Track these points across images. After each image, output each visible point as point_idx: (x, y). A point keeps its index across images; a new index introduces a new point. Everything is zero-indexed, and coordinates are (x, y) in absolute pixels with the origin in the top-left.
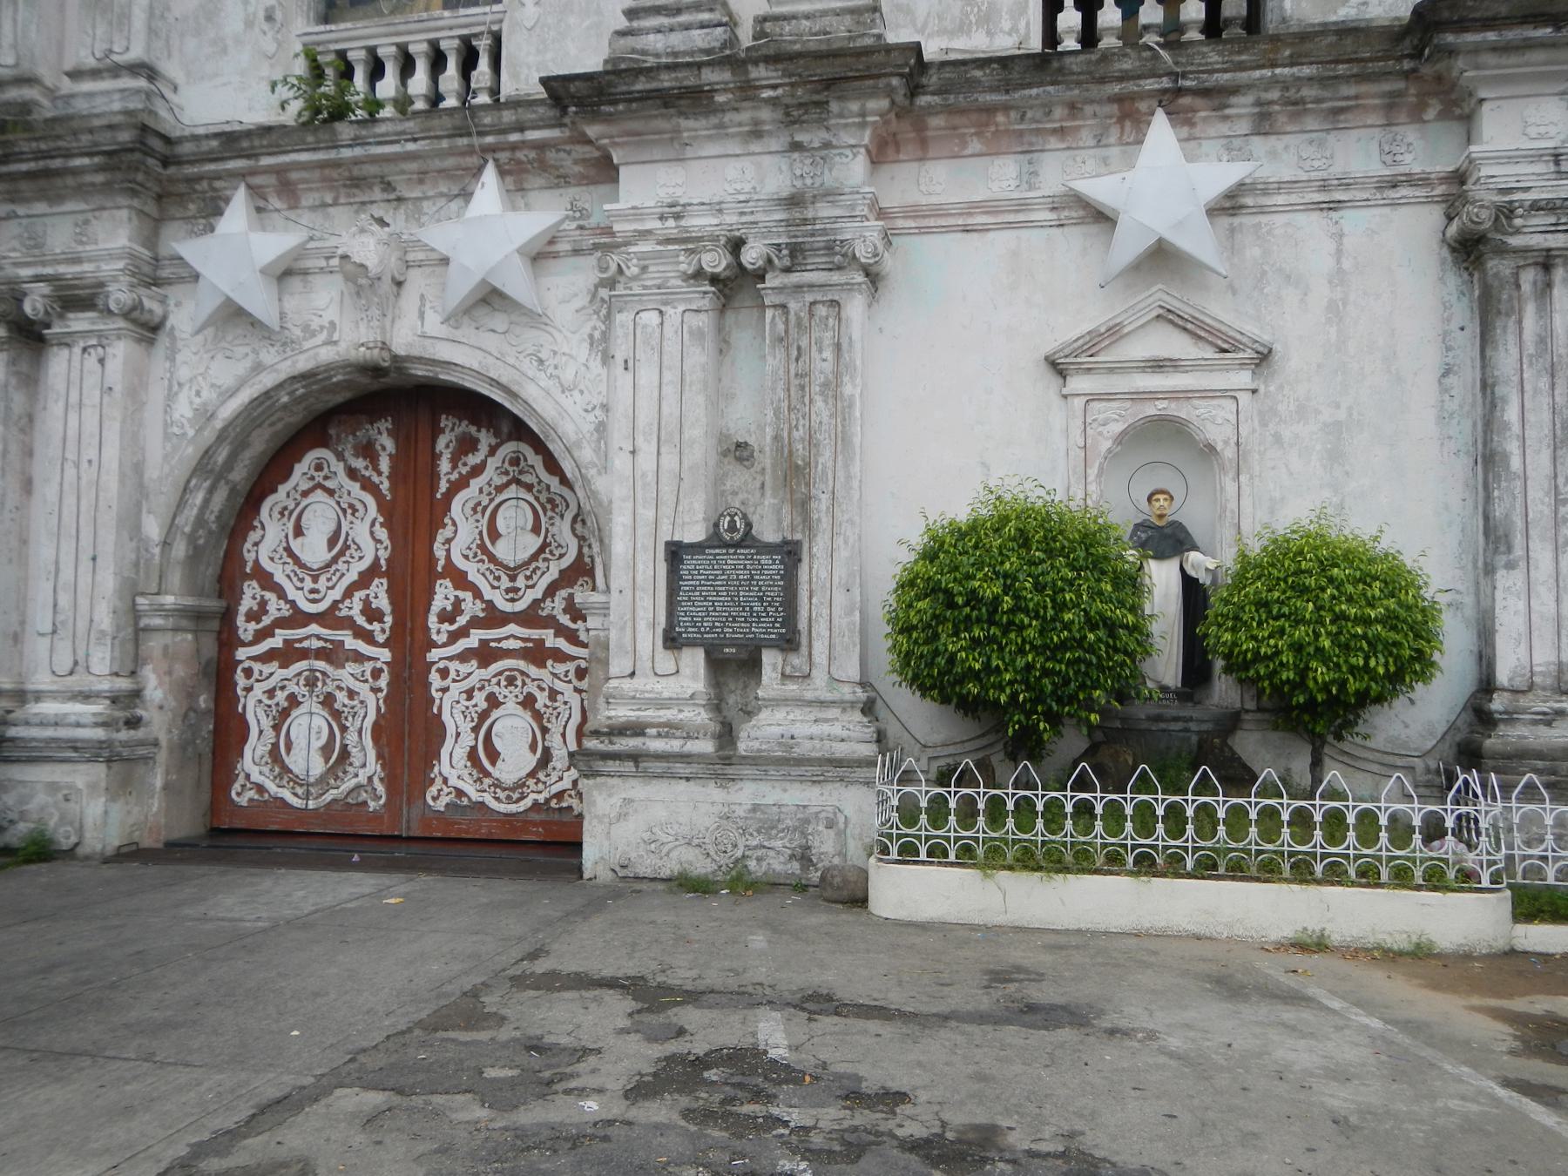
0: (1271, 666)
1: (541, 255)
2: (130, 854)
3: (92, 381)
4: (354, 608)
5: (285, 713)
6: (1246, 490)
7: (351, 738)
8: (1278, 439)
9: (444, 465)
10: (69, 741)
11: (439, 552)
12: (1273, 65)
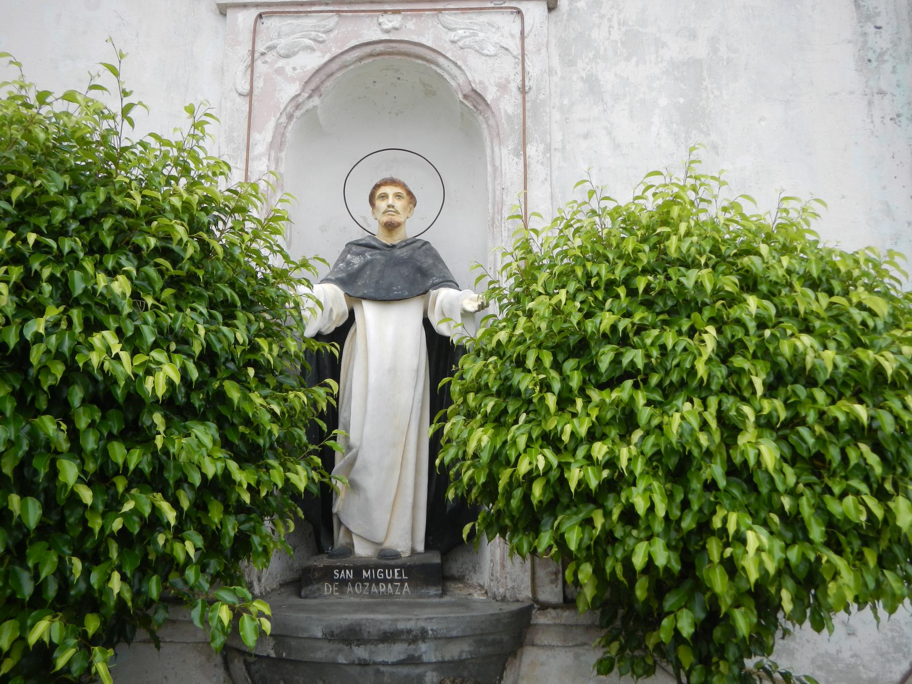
0: (599, 521)
6: (538, 171)
8: (593, 85)
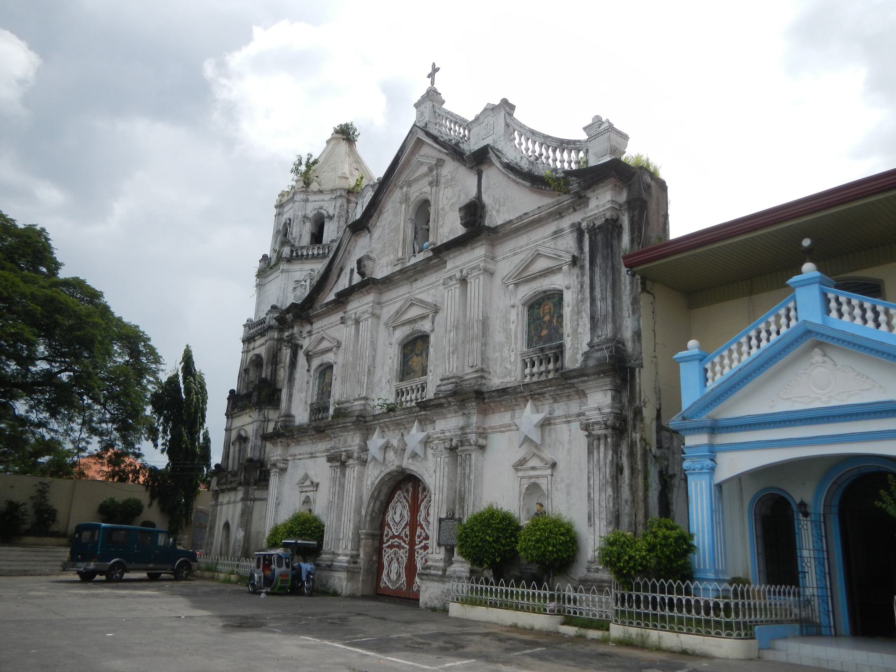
1: (426, 442)
2: (352, 597)
3: (352, 476)
4: (403, 535)
5: (390, 562)
7: (401, 570)
9: (420, 496)
10: (340, 566)
11: (418, 519)
12: (547, 387)
